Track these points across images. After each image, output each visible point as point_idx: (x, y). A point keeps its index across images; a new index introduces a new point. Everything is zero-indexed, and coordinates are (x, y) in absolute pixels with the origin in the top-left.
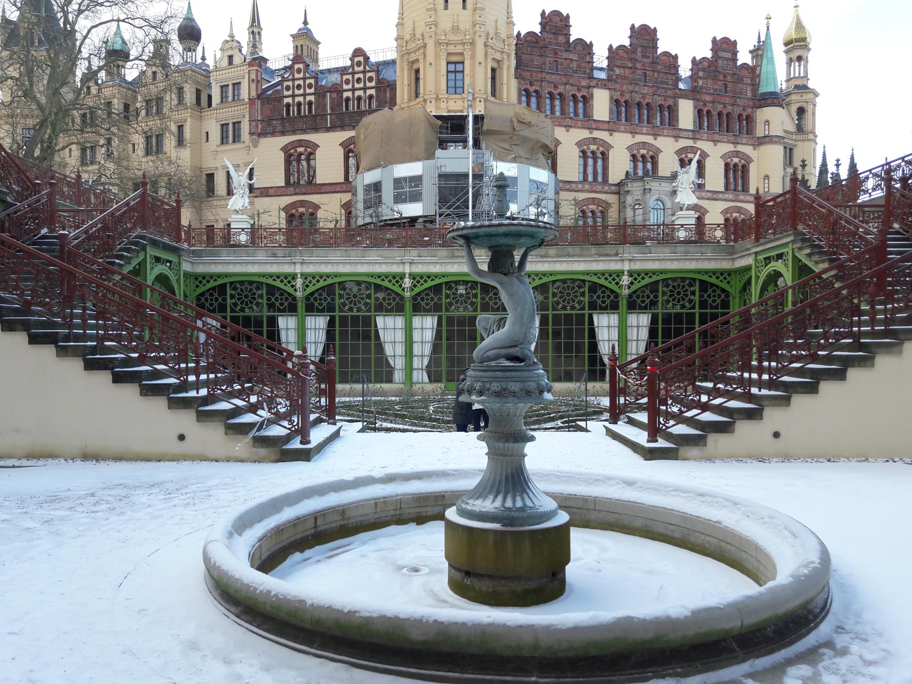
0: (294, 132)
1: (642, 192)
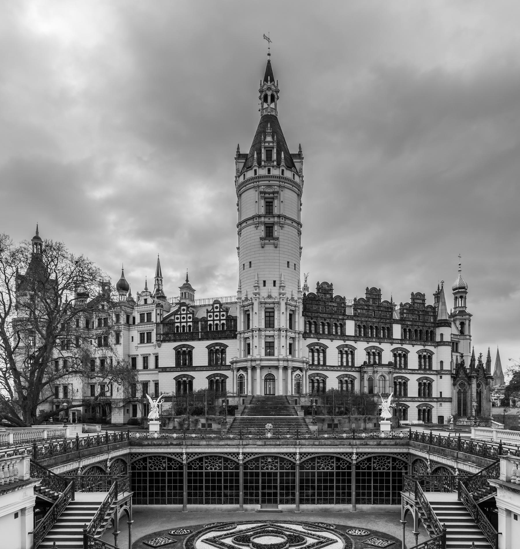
0: (181, 340)
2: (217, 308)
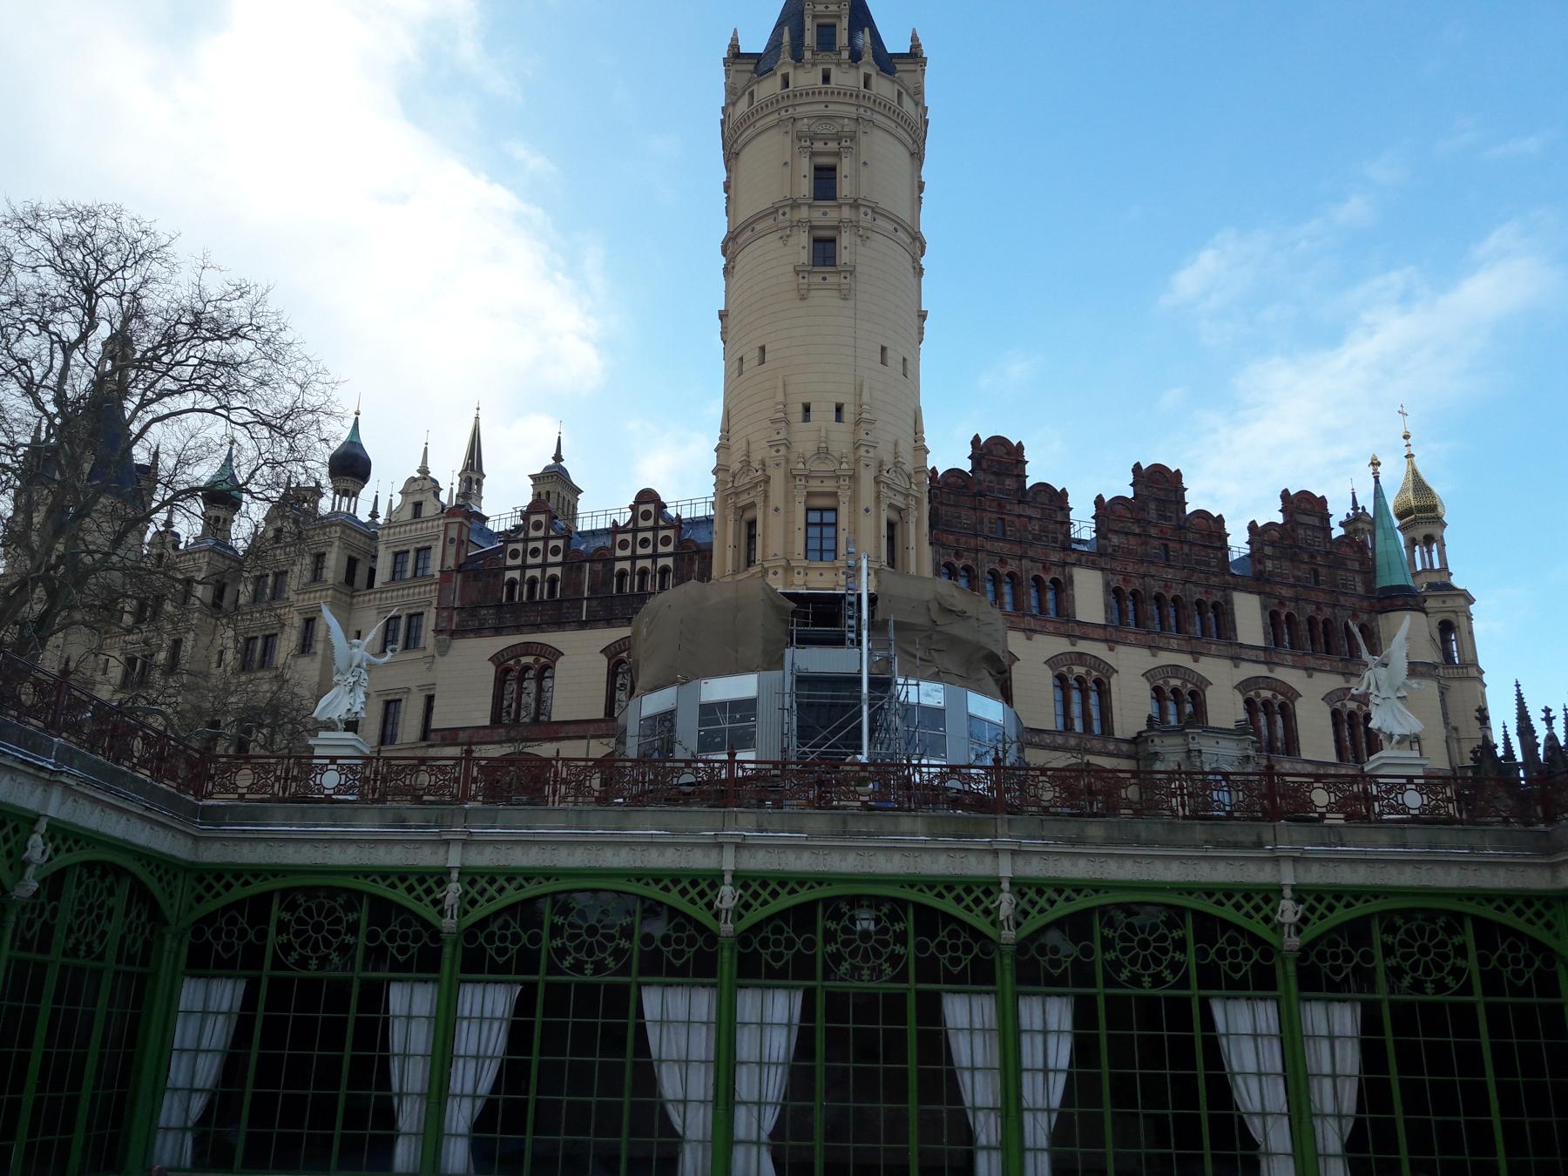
0: (518, 629)
1: (1184, 755)
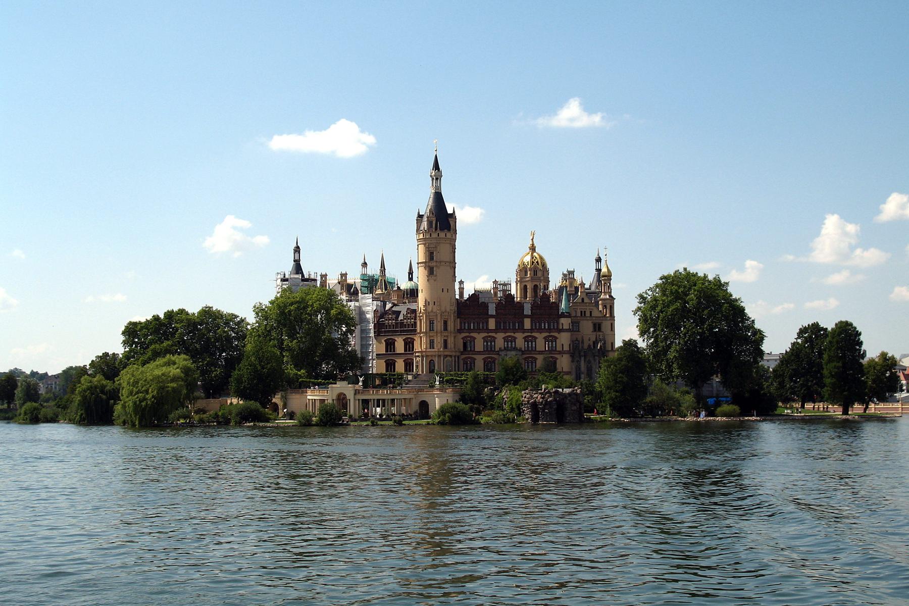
2: (409, 313)
